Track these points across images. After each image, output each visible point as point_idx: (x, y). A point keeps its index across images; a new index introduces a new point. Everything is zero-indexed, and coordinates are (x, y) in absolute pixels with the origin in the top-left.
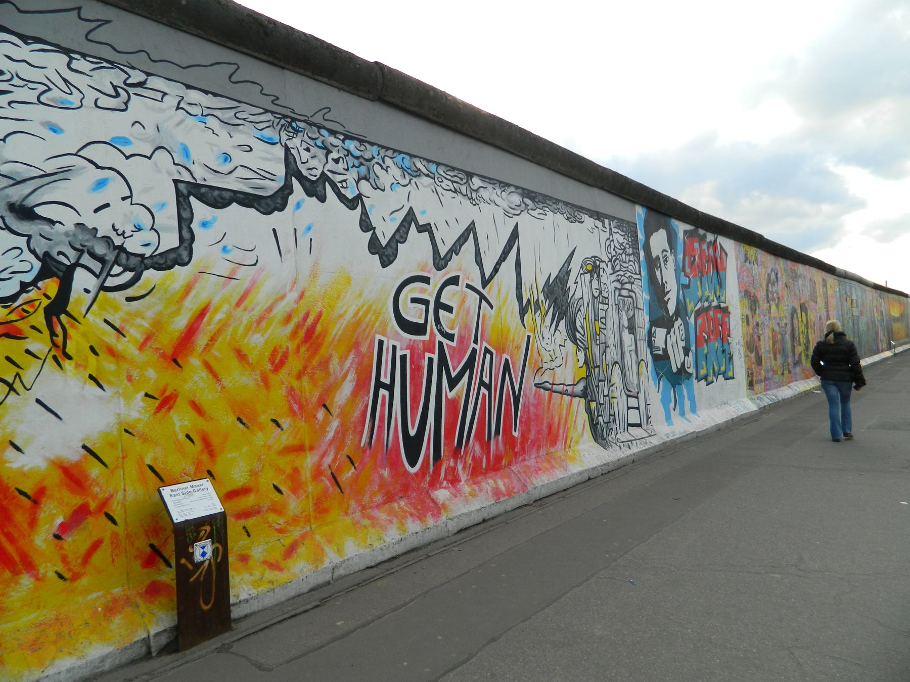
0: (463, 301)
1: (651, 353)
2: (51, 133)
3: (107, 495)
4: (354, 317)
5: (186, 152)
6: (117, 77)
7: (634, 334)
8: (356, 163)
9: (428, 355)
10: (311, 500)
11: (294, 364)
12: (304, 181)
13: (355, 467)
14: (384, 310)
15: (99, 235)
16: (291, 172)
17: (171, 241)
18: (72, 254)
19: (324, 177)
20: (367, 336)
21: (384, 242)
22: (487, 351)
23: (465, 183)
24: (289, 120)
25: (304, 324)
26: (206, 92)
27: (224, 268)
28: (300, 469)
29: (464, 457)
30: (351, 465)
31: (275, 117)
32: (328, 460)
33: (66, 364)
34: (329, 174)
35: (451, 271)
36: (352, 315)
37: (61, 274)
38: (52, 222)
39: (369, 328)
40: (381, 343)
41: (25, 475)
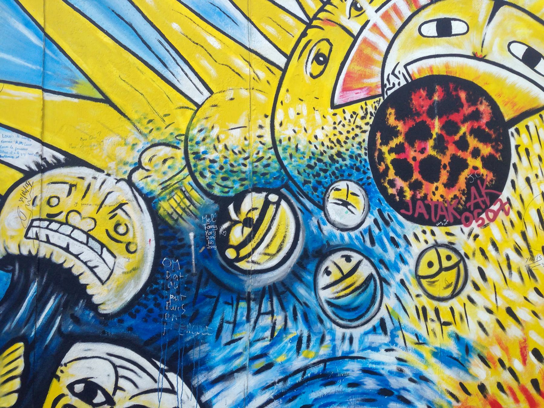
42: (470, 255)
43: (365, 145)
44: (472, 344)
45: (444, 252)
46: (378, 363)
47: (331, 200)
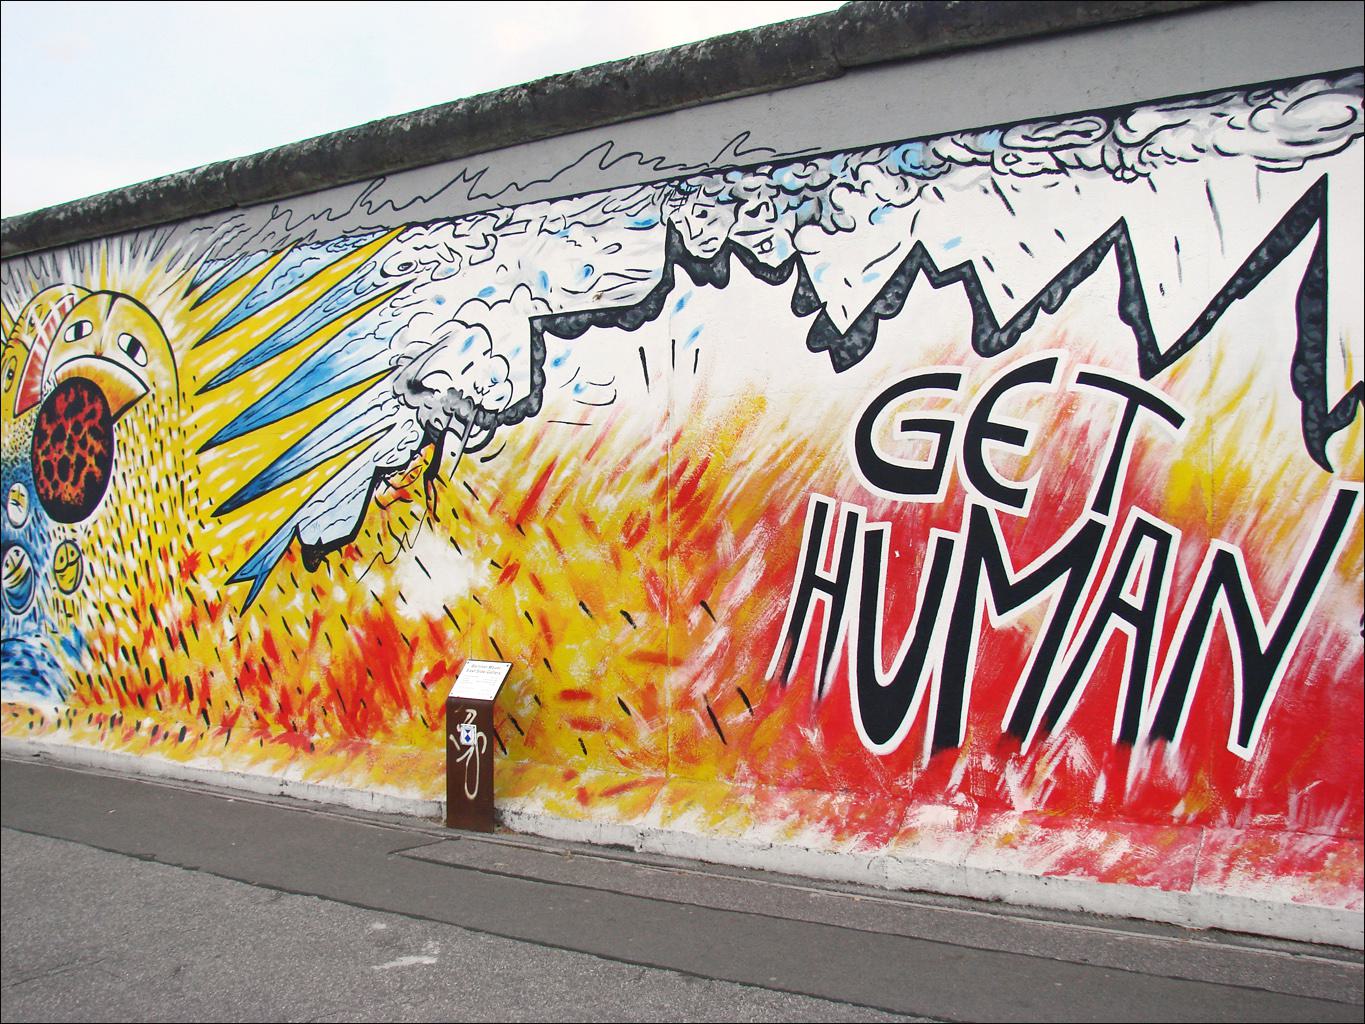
0: (1065, 413)
2: (438, 305)
3: (458, 659)
4: (765, 466)
5: (544, 281)
6: (486, 226)
8: (794, 201)
9: (935, 534)
10: (671, 737)
11: (658, 538)
12: (693, 264)
13: (751, 710)
14: (834, 449)
15: (464, 397)
16: (674, 258)
17: (523, 390)
18: (444, 419)
19: (729, 247)
20: (792, 497)
21: (843, 326)
22: (1142, 528)
23: (1096, 140)
24: (676, 183)
25: (678, 480)
26: (570, 198)
27: (574, 413)
28: (657, 687)
29: (1030, 760)
30: (745, 705)
31: (657, 188)
32: (703, 687)
33: (436, 525)
34: (739, 240)
35: (1029, 349)
36: (765, 461)
37: (436, 439)
38: (432, 391)
39: (797, 482)
40: (821, 509)
41: (408, 624)
42: (85, 550)
43: (29, 449)
44: (84, 636)
45: (71, 548)
46: (31, 647)
47: (11, 501)
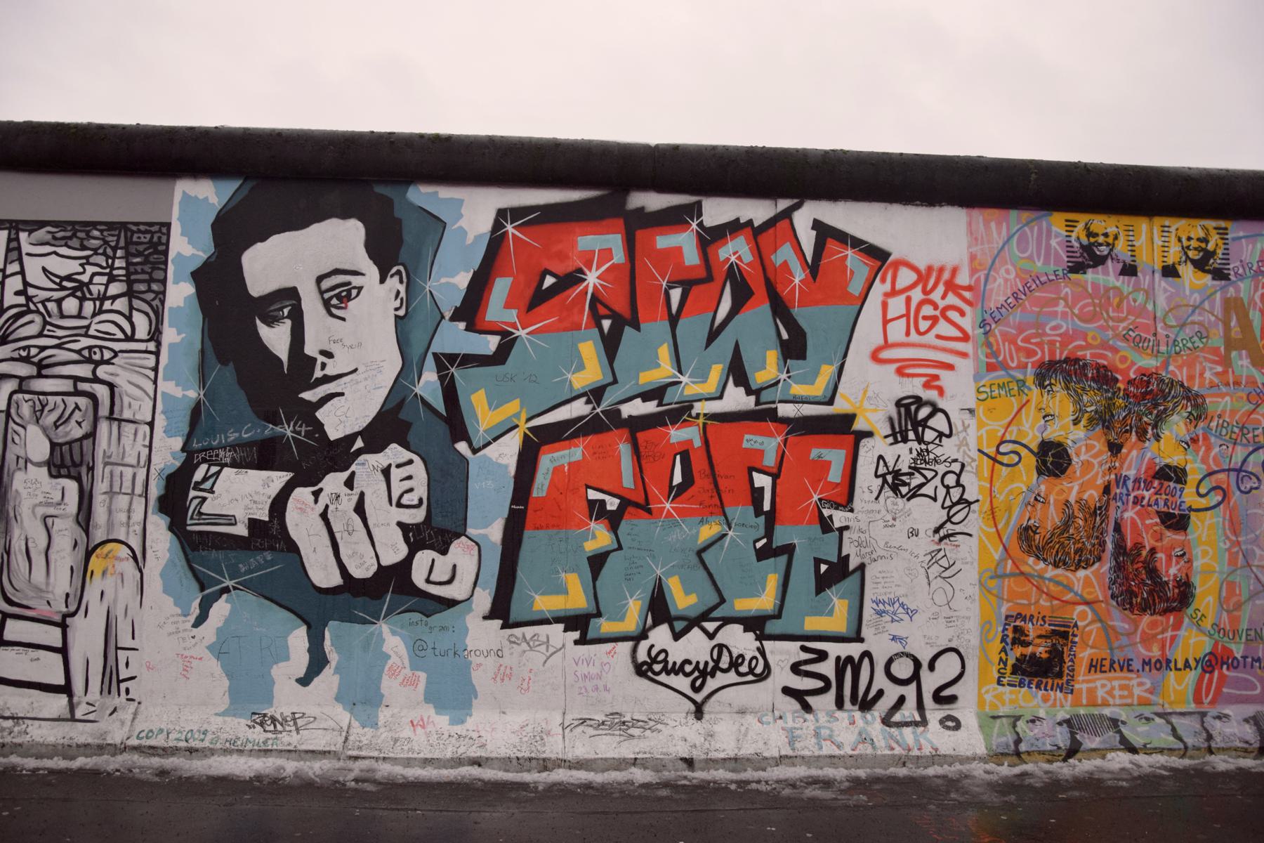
1: (177, 527)
7: (78, 479)
